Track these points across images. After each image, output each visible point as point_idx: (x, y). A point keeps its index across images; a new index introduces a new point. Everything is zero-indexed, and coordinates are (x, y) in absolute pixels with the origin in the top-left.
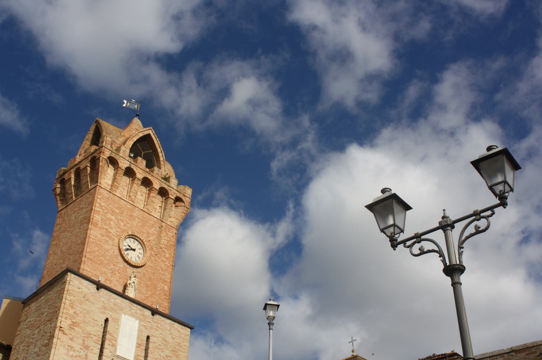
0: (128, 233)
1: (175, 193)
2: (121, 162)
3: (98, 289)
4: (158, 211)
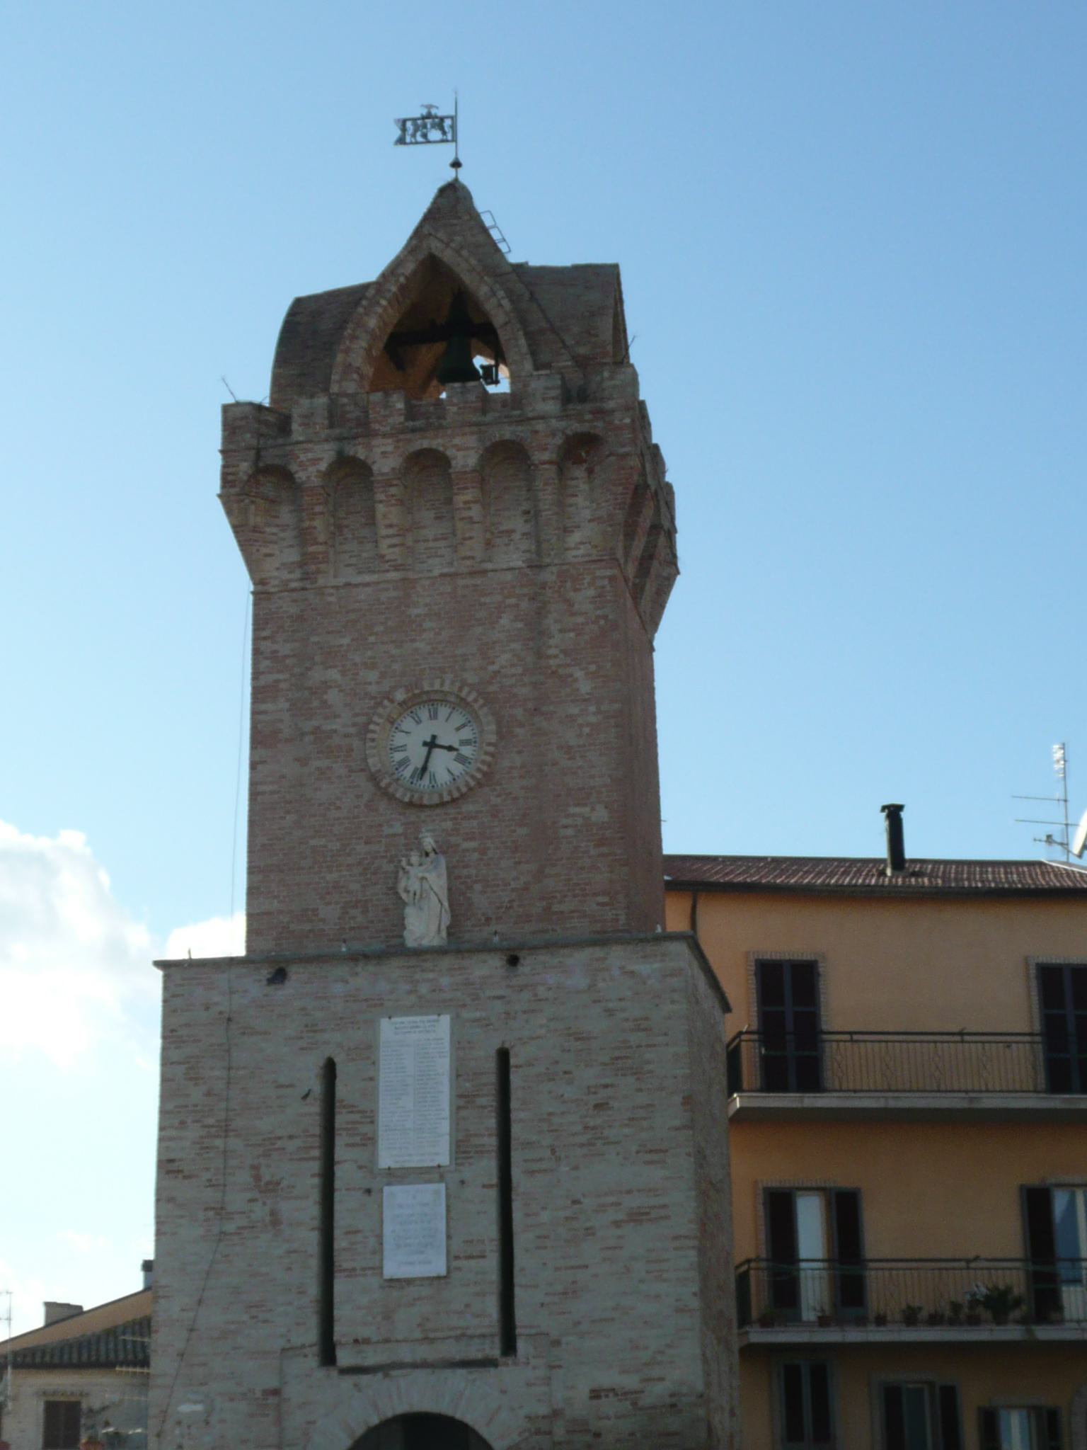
0: (392, 701)
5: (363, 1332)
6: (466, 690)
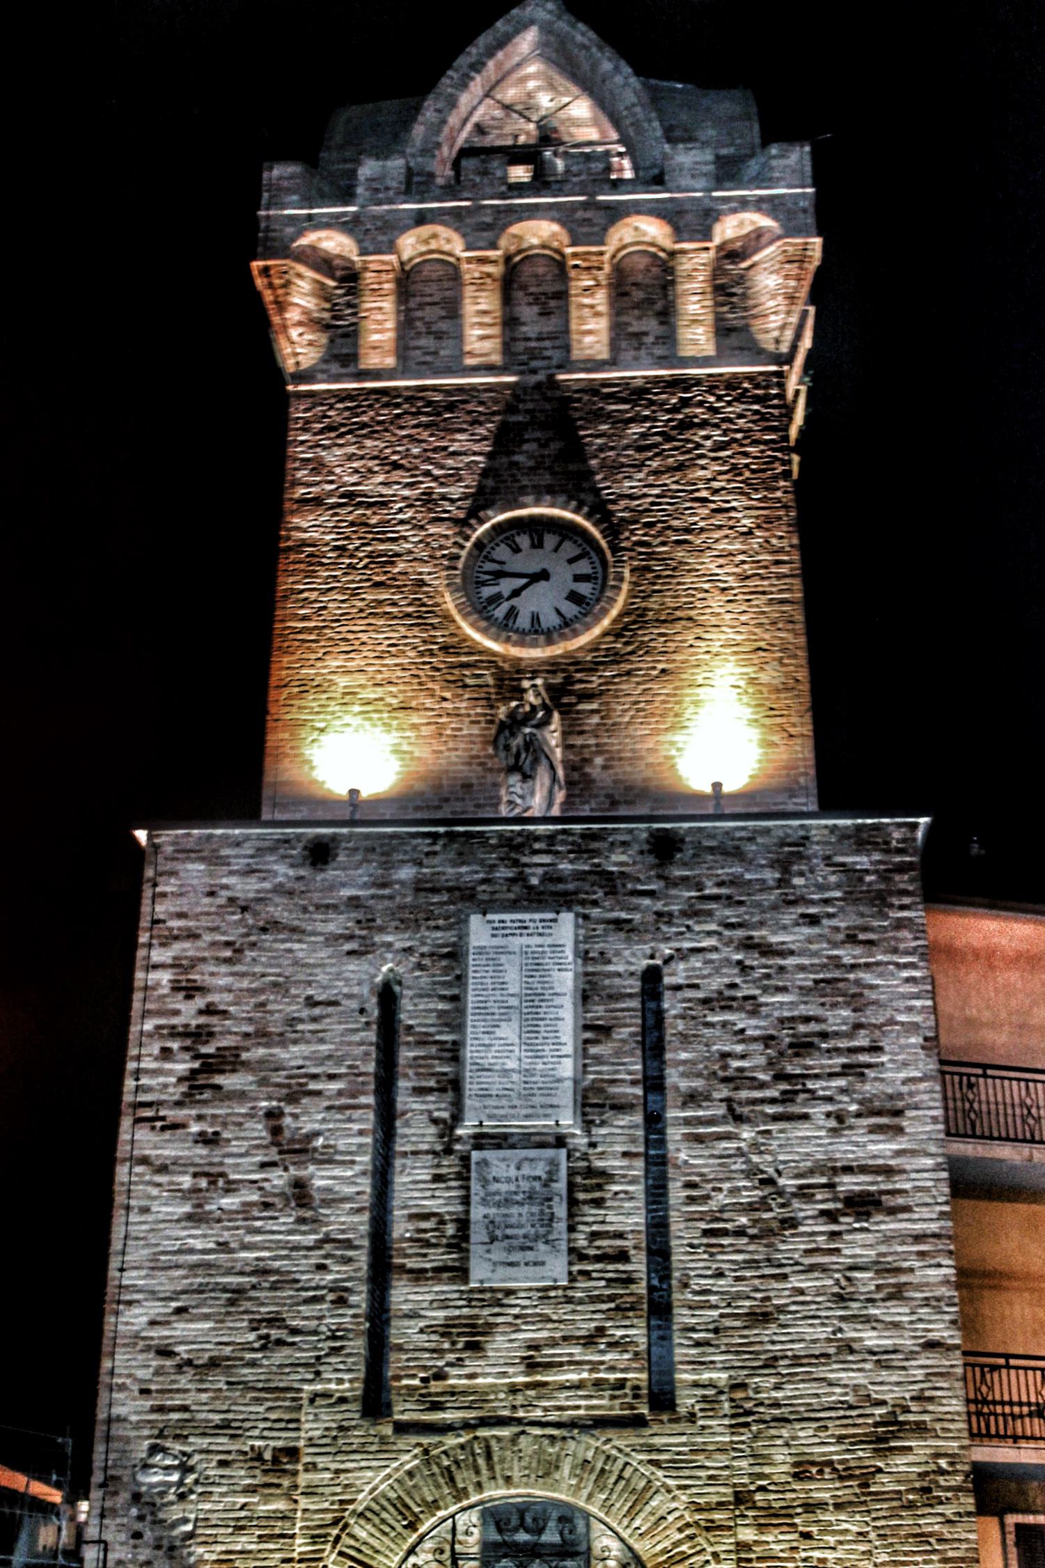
4: (657, 338)
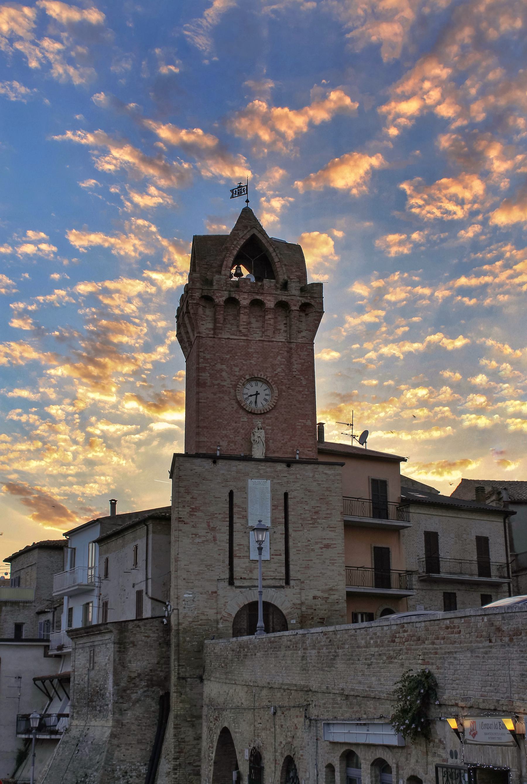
0: (245, 378)
1: (298, 301)
2: (217, 297)
3: (215, 462)
5: (244, 576)
6: (268, 378)
